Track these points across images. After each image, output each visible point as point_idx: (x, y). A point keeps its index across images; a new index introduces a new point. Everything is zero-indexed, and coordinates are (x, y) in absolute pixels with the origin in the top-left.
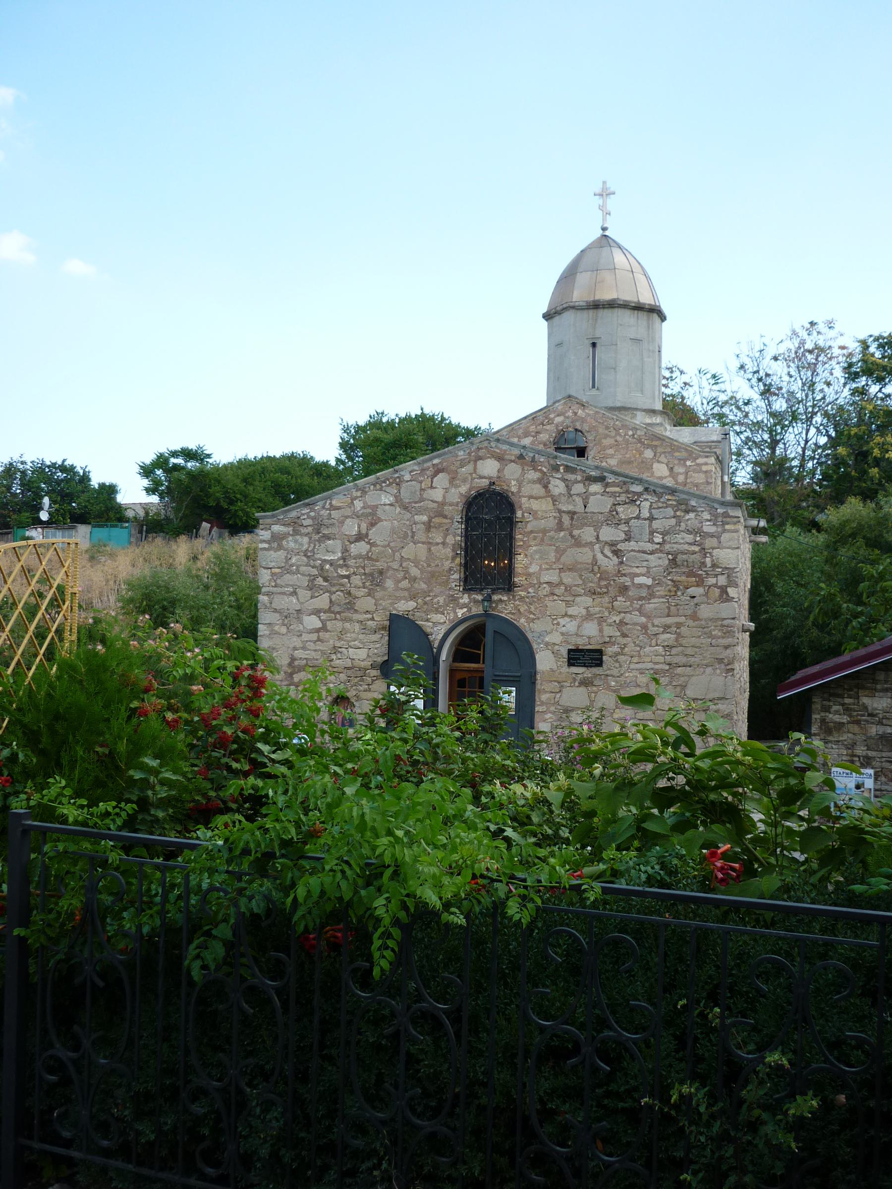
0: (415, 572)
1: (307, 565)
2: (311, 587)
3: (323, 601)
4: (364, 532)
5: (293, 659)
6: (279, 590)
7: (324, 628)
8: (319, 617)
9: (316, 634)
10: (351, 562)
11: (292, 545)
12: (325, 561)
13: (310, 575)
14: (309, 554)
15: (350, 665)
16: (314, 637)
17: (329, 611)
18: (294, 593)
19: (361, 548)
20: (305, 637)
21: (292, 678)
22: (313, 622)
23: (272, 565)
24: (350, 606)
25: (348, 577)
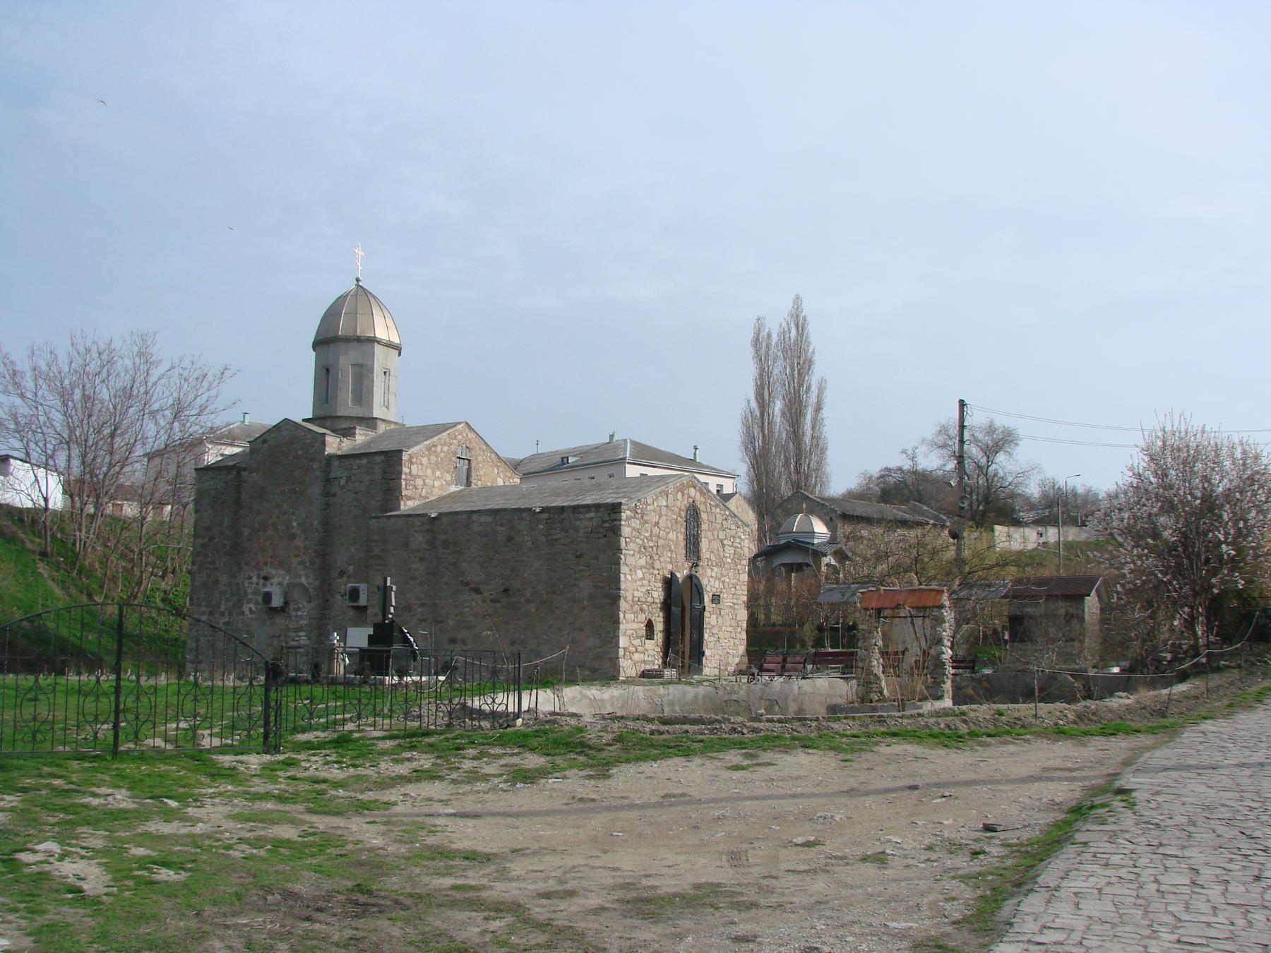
2: (640, 552)
3: (643, 562)
7: (643, 578)
16: (639, 583)
19: (656, 530)
22: (640, 574)
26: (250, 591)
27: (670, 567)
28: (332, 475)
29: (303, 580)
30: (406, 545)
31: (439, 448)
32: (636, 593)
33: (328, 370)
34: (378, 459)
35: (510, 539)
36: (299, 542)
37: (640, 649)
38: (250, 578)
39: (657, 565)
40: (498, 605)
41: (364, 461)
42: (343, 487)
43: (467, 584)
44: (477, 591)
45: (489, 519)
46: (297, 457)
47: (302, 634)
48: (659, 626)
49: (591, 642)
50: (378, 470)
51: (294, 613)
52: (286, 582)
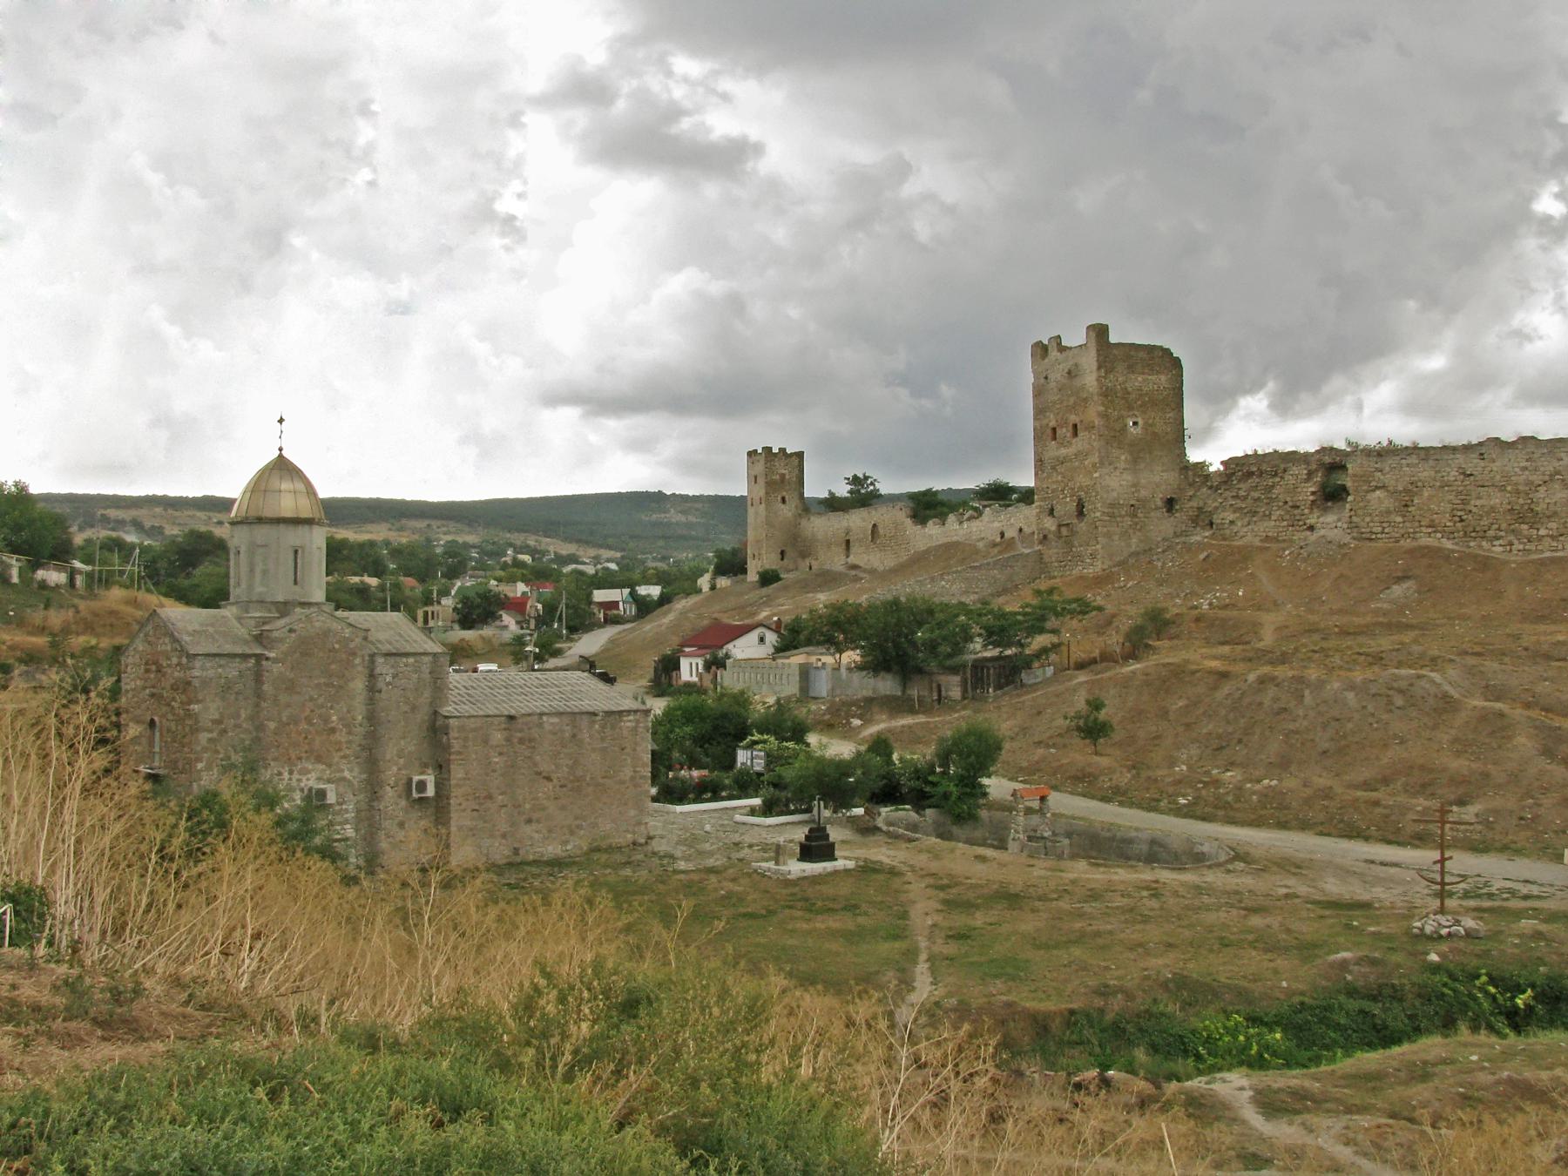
28: (378, 671)
29: (347, 774)
30: (486, 742)
33: (296, 552)
34: (426, 659)
35: (574, 736)
36: (341, 736)
38: (280, 774)
41: (411, 660)
42: (389, 684)
44: (548, 779)
45: (555, 720)
46: (333, 650)
49: (632, 813)
50: (426, 669)
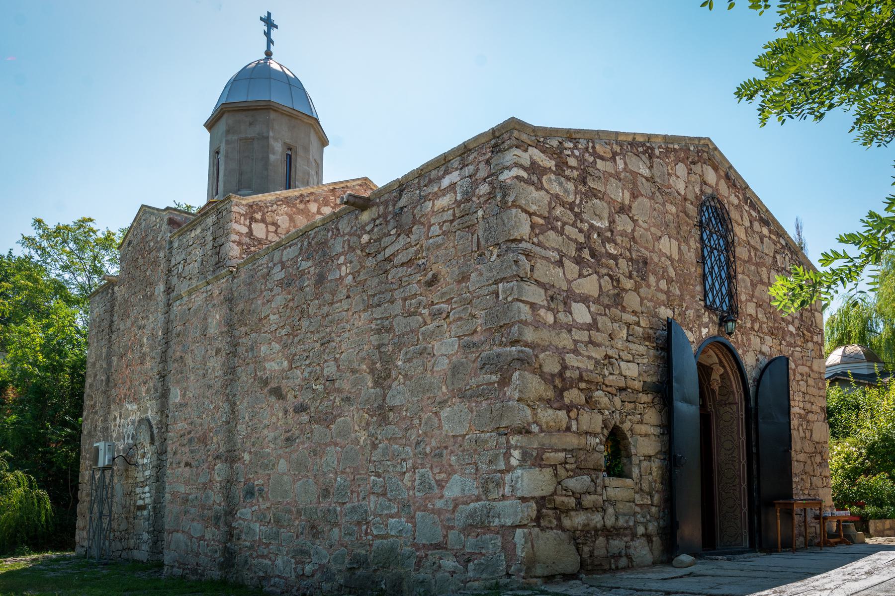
0: (672, 273)
1: (574, 225)
2: (579, 261)
4: (627, 202)
5: (565, 367)
6: (543, 252)
7: (593, 326)
8: (588, 307)
9: (586, 333)
10: (619, 239)
11: (556, 189)
12: (592, 226)
13: (576, 241)
14: (576, 210)
15: (623, 385)
16: (583, 336)
17: (597, 301)
18: (560, 264)
20: (578, 335)
21: (562, 397)
23: (533, 208)
24: (617, 300)
25: (615, 258)
26: (114, 435)
27: (665, 313)
28: (173, 262)
31: (313, 207)
32: (572, 360)
36: (148, 364)
37: (588, 500)
38: (115, 418)
39: (632, 300)
40: (305, 418)
43: (266, 382)
44: (277, 393)
47: (147, 489)
48: (645, 443)
51: (140, 461)
52: (137, 419)
